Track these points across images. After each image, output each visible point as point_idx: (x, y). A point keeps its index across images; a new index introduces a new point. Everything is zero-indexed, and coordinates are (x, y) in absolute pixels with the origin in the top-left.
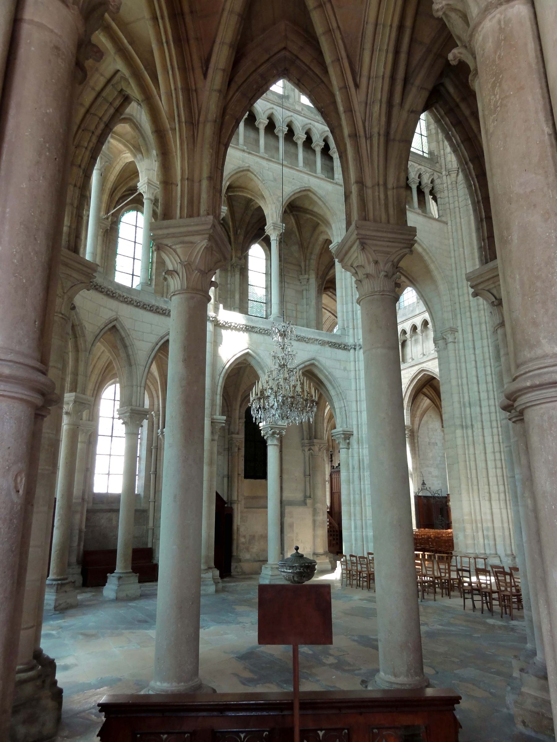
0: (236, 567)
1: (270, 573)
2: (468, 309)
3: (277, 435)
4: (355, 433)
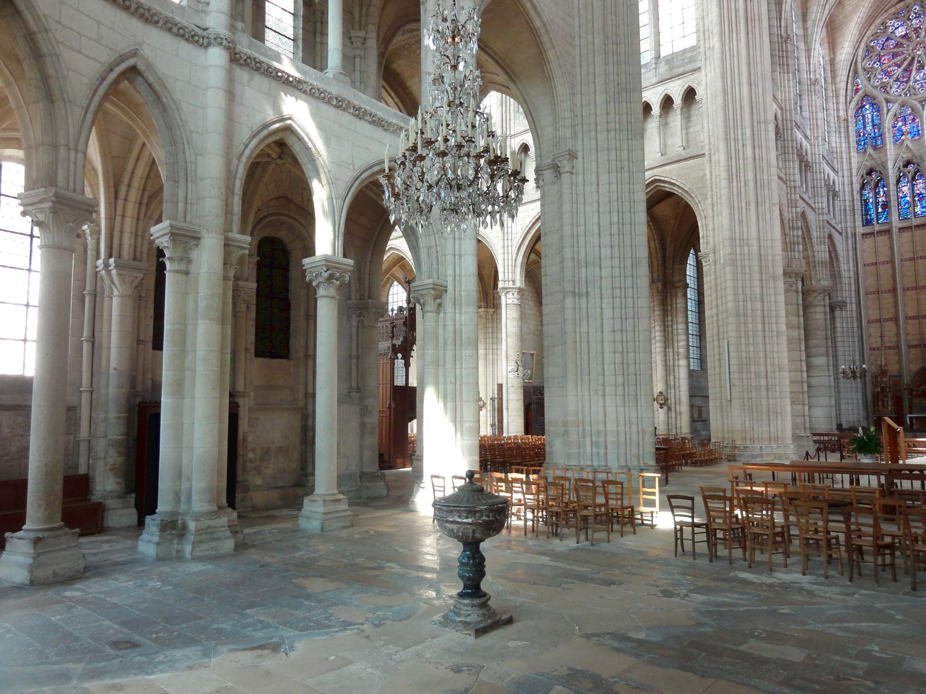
0: (243, 500)
1: (321, 509)
2: (593, 126)
3: (337, 280)
4: (450, 288)
